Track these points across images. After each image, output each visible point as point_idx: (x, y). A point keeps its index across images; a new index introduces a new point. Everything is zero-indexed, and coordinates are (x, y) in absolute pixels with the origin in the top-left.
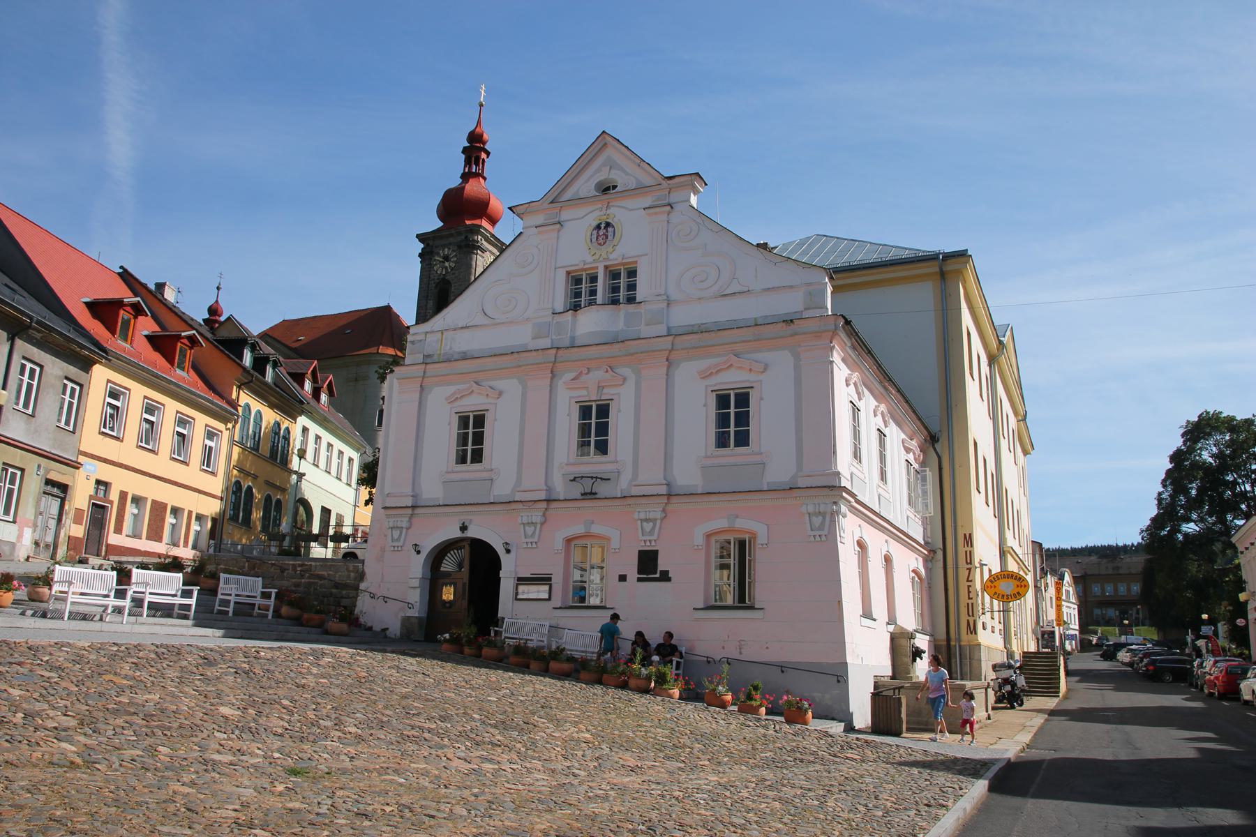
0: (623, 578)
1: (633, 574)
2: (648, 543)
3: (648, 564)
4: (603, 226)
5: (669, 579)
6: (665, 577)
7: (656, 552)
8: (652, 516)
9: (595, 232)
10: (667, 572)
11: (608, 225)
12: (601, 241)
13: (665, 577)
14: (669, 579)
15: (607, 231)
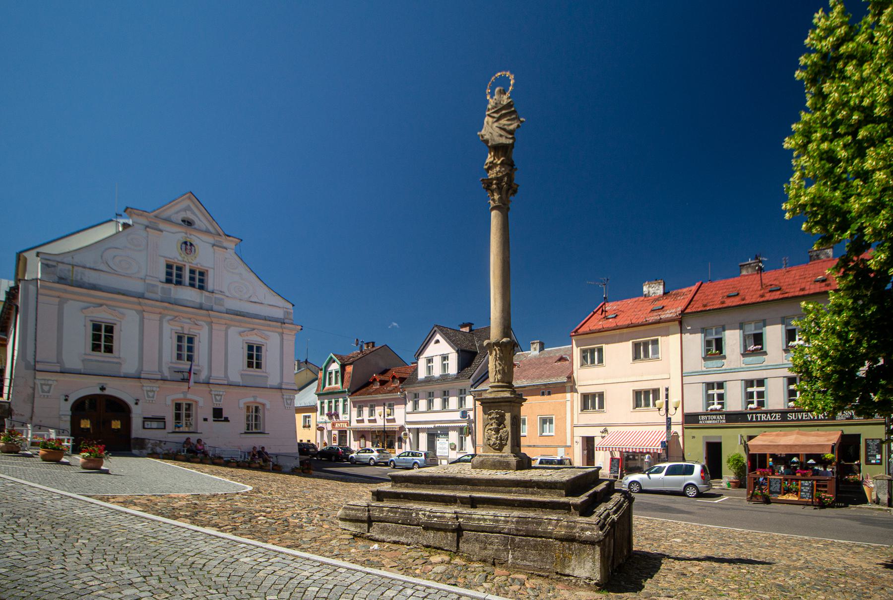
0: (205, 420)
1: (211, 418)
3: (218, 414)
4: (189, 244)
5: (229, 421)
6: (226, 420)
8: (221, 393)
9: (184, 245)
10: (227, 418)
11: (191, 245)
12: (188, 251)
13: (226, 420)
14: (229, 421)
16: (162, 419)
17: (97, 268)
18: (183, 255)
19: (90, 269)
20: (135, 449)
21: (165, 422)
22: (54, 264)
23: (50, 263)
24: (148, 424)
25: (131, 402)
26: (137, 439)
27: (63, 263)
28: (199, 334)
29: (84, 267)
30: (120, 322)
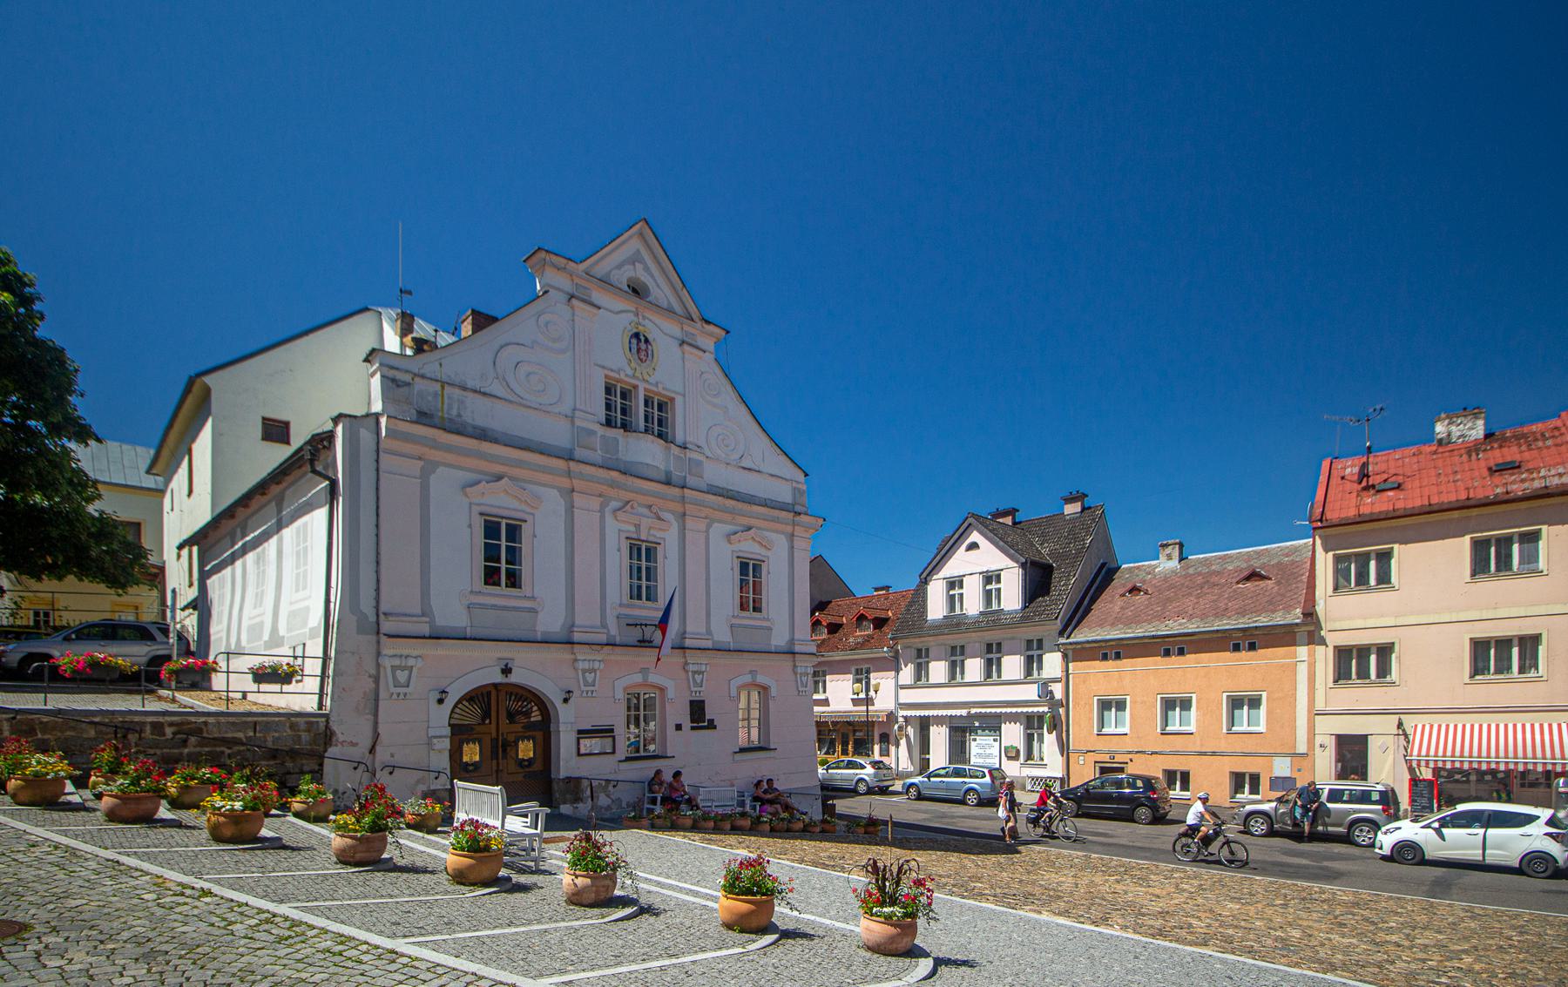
0: (679, 727)
1: (687, 724)
2: (698, 694)
5: (715, 727)
7: (703, 702)
11: (647, 341)
14: (715, 727)
15: (647, 347)
16: (606, 732)
17: (487, 390)
18: (633, 365)
19: (475, 391)
20: (565, 803)
21: (614, 737)
22: (407, 378)
23: (400, 376)
24: (588, 744)
25: (552, 693)
26: (569, 780)
27: (423, 377)
28: (664, 539)
29: (464, 389)
30: (533, 515)
